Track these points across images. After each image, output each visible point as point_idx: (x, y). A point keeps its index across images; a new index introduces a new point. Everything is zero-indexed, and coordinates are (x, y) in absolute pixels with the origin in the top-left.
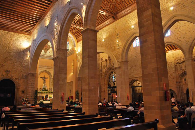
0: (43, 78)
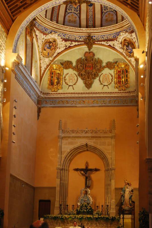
0: (82, 172)
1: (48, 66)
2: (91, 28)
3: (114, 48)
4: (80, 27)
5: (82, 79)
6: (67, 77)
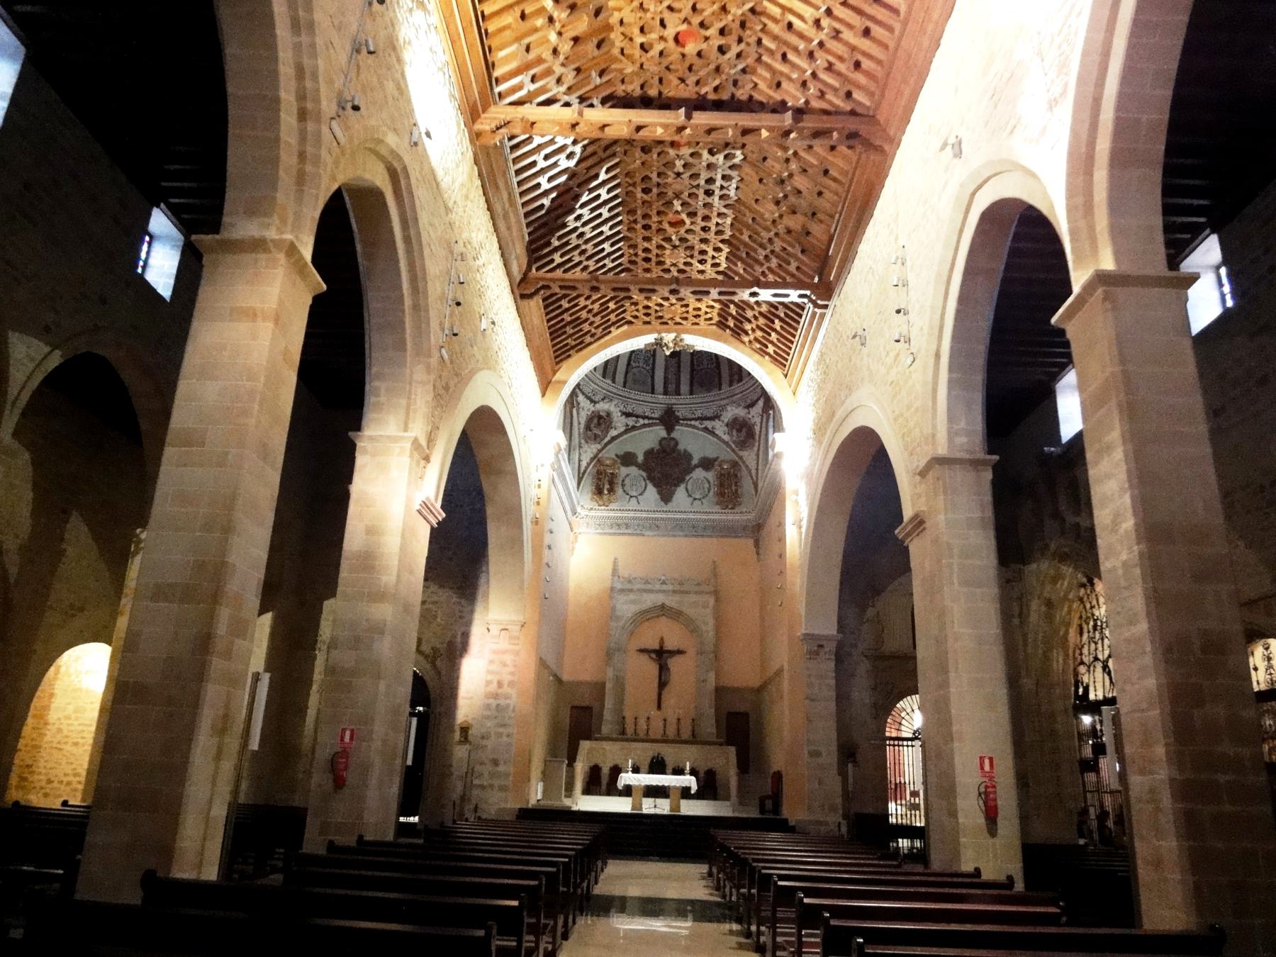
1: (592, 459)
2: (672, 395)
3: (712, 433)
4: (653, 392)
5: (655, 485)
6: (627, 481)
